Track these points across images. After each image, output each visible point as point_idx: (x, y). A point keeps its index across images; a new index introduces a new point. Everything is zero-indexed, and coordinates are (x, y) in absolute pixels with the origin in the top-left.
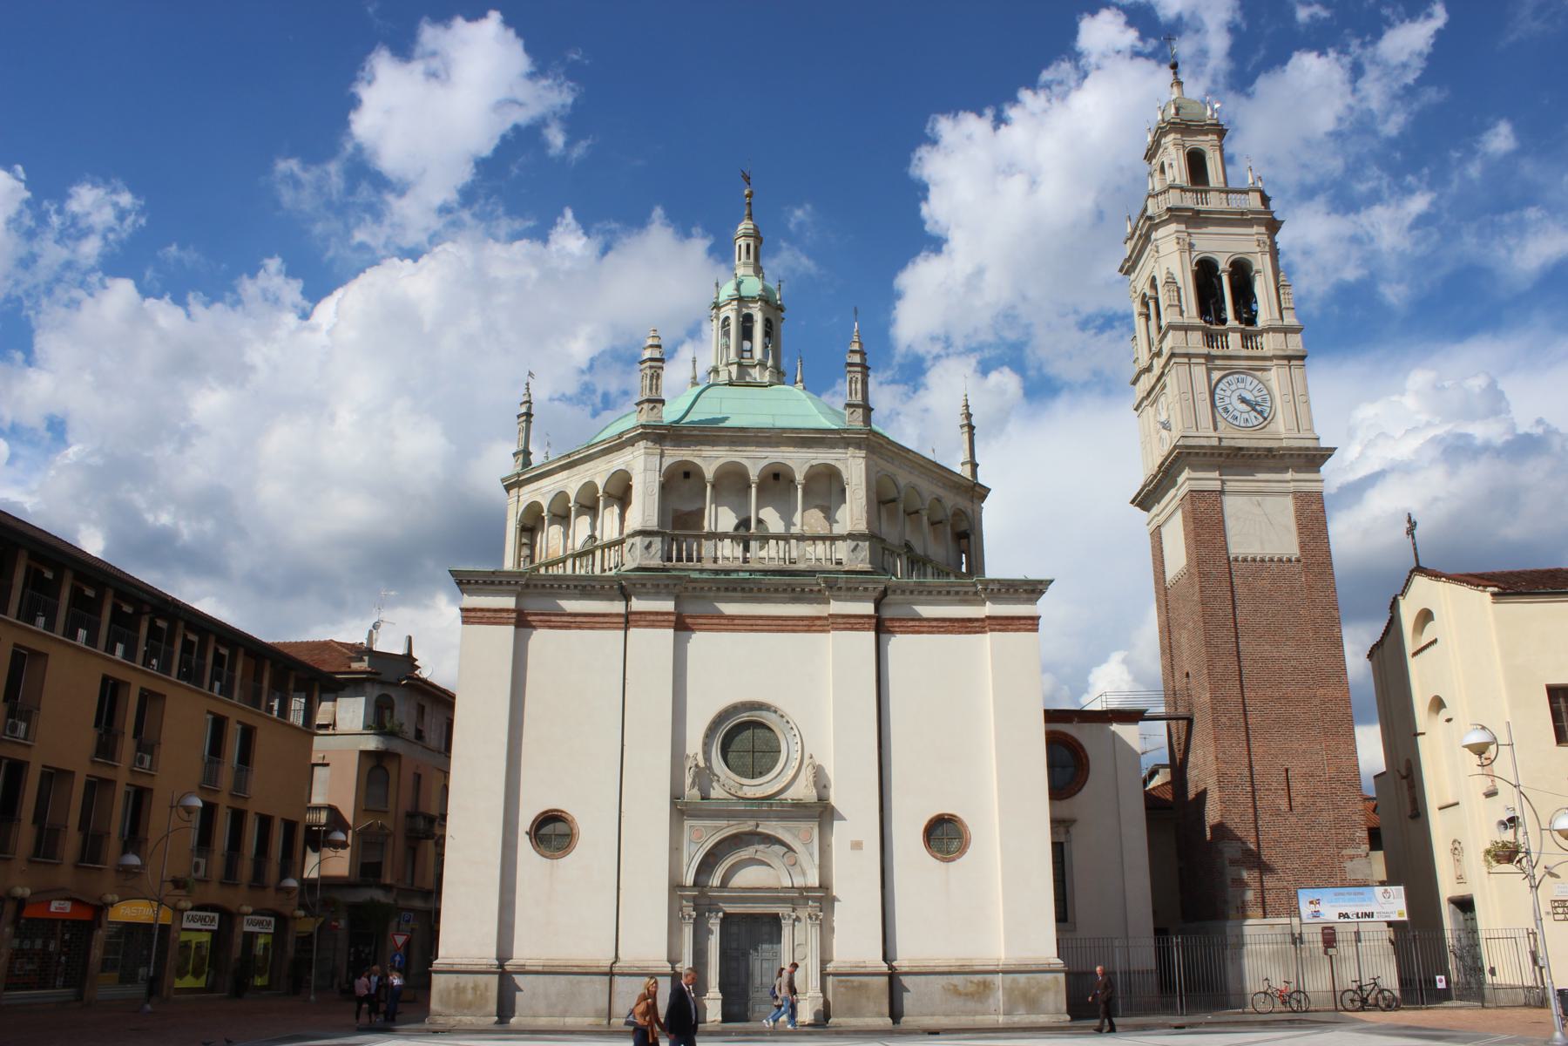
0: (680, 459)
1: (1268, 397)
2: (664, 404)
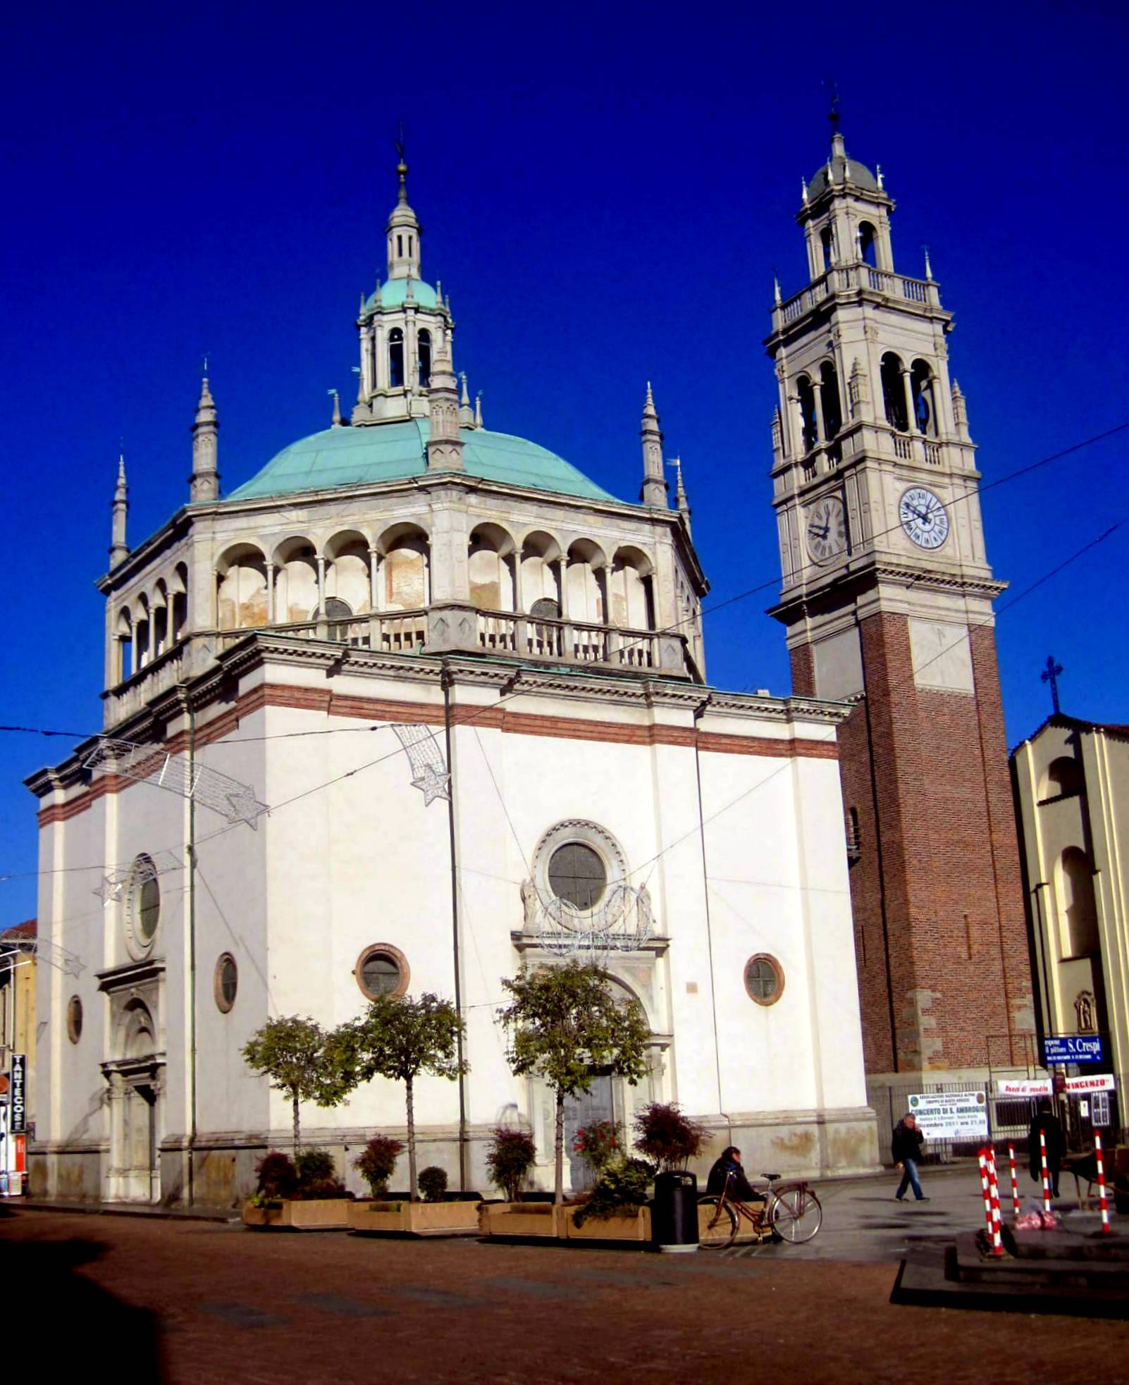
0: (486, 521)
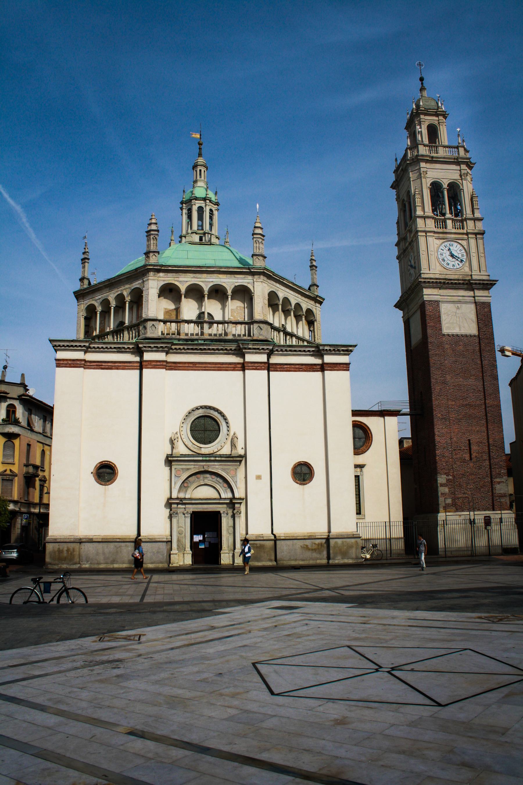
1: (465, 254)
2: (159, 254)
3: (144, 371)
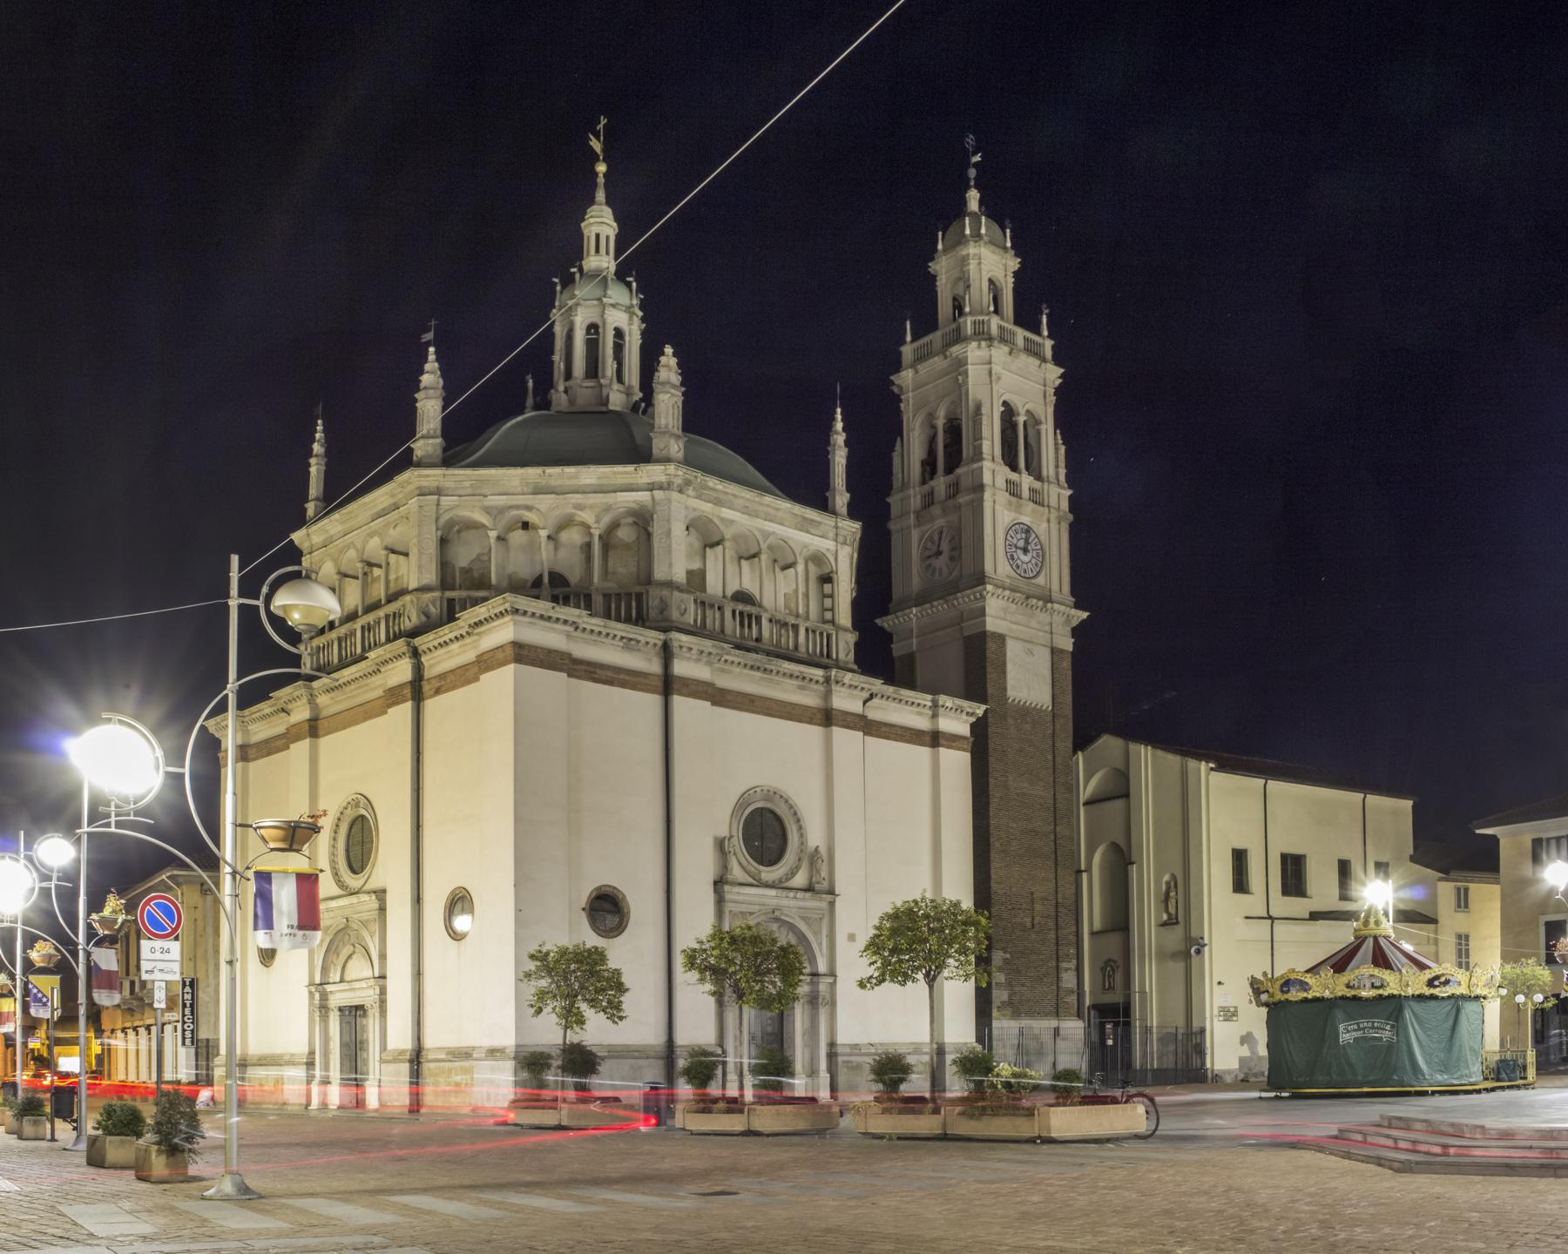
3: (678, 701)
